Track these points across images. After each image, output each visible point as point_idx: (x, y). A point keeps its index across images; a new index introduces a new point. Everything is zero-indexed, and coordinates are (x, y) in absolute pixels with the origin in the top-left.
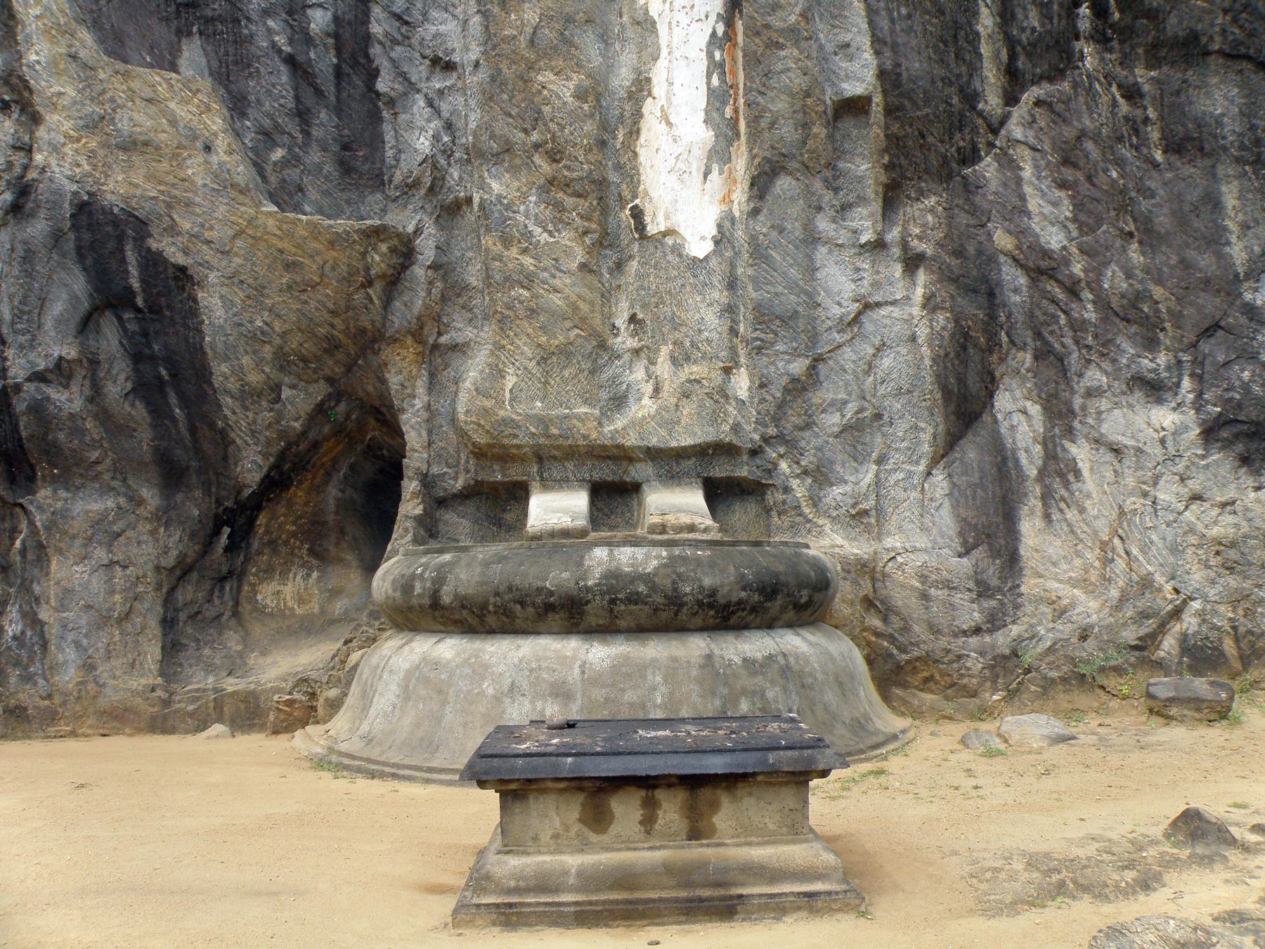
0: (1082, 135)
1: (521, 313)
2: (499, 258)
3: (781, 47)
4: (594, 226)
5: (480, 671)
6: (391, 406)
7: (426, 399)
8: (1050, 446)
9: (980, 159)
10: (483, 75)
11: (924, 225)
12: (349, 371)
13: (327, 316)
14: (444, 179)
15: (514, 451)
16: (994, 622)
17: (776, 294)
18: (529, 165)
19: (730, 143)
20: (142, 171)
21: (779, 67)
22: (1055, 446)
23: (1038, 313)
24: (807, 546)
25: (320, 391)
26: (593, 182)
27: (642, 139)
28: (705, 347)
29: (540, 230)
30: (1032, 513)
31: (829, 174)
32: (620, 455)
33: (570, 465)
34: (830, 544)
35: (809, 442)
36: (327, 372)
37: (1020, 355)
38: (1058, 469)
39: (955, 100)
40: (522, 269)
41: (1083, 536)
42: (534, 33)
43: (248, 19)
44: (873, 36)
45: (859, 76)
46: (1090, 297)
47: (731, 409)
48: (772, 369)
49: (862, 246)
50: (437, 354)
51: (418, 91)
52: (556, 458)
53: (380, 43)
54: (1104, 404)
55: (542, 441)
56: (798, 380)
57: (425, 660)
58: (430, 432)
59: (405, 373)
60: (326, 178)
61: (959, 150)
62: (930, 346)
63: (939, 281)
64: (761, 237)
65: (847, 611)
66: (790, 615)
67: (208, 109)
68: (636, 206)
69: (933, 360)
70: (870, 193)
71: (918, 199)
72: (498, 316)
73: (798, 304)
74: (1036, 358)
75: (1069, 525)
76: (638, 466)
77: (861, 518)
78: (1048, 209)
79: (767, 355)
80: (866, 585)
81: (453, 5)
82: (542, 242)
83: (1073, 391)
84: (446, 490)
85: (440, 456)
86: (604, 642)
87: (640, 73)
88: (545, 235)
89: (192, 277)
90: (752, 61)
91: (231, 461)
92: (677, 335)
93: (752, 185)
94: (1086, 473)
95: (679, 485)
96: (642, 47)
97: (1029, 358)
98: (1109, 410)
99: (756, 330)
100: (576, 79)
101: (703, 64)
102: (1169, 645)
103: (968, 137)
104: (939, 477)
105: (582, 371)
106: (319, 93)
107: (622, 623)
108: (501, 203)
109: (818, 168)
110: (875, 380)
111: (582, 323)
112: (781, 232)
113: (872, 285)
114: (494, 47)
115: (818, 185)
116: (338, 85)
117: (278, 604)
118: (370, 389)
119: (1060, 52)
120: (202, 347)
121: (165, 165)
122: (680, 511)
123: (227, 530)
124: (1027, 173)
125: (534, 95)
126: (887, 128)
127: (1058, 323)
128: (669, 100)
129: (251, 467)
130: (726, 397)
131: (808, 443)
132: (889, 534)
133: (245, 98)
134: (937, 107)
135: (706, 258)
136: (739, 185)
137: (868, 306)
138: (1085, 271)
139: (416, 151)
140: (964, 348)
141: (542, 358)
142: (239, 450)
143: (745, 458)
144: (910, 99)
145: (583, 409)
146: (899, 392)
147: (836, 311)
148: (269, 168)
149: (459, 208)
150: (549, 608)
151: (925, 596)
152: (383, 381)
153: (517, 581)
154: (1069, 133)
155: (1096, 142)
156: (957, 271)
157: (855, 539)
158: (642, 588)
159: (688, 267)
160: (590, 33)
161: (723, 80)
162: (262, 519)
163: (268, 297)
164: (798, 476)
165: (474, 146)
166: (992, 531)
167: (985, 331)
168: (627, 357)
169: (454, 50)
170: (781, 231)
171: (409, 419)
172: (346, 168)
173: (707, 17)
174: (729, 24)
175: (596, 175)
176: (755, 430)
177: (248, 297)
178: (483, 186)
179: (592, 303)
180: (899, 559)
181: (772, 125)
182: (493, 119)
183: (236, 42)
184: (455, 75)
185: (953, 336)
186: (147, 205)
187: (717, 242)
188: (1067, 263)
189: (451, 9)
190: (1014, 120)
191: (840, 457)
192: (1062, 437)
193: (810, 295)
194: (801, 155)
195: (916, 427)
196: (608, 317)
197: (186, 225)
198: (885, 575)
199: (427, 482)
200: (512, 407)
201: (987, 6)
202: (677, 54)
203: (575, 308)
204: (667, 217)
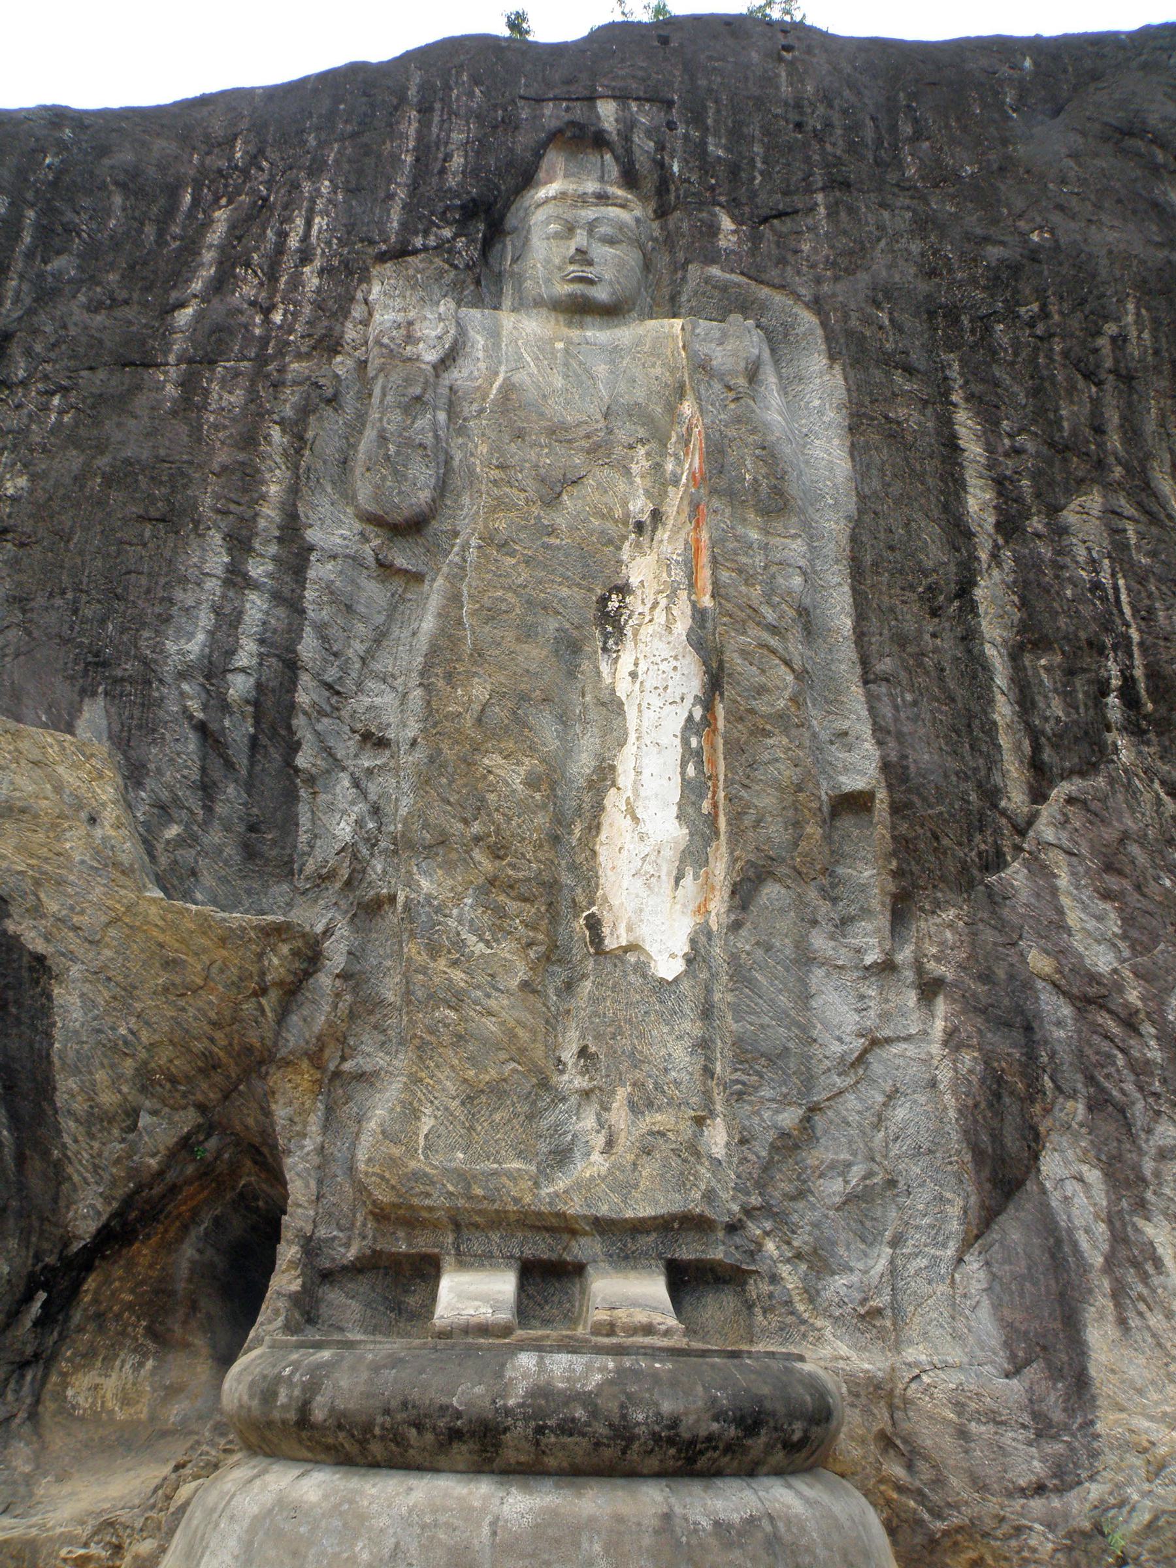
0: (1125, 837)
1: (446, 1039)
2: (424, 970)
3: (768, 734)
4: (541, 937)
5: (353, 1522)
6: (274, 1146)
7: (319, 1139)
8: (1118, 1224)
9: (1006, 865)
10: (420, 755)
11: (942, 944)
12: (226, 1097)
13: (207, 1028)
14: (364, 871)
15: (425, 1214)
17: (762, 1026)
18: (467, 861)
20: (13, 842)
21: (766, 756)
22: (1124, 1225)
23: (1088, 1051)
24: (801, 1358)
25: (187, 1120)
26: (543, 884)
27: (603, 836)
28: (671, 1091)
29: (475, 939)
31: (825, 881)
32: (562, 1227)
33: (495, 1237)
34: (832, 1356)
35: (803, 1215)
36: (199, 1097)
37: (1070, 1104)
38: (1132, 1258)
39: (973, 797)
40: (450, 985)
42: (483, 711)
43: (161, 681)
44: (875, 723)
45: (860, 769)
46: (1153, 1031)
47: (703, 1171)
48: (756, 1120)
49: (867, 968)
50: (337, 1083)
51: (344, 769)
52: (477, 1227)
53: (305, 713)
55: (461, 1202)
56: (789, 1135)
57: (281, 1502)
58: (320, 1182)
59: (296, 1104)
60: (226, 862)
61: (980, 854)
62: (954, 1093)
63: (964, 1012)
64: (744, 956)
65: (857, 1452)
66: (779, 1456)
67: (101, 776)
68: (593, 915)
69: (960, 1111)
70: (875, 904)
71: (933, 912)
72: (417, 1042)
73: (789, 1039)
74: (1090, 1108)
76: (583, 1241)
77: (873, 1319)
78: (1091, 924)
79: (750, 1103)
80: (881, 1413)
81: (393, 676)
82: (477, 953)
83: (1141, 1152)
84: (334, 1260)
85: (330, 1215)
86: (526, 1489)
87: (604, 760)
88: (481, 945)
89: (50, 968)
90: (734, 749)
91: (62, 1203)
92: (638, 1074)
93: (733, 893)
95: (634, 1268)
96: (606, 731)
97: (1081, 1108)
99: (736, 1070)
100: (529, 763)
101: (676, 752)
103: (990, 840)
104: (973, 1264)
105: (516, 1115)
106: (229, 765)
107: (551, 1462)
108: (430, 905)
109: (813, 874)
111: (520, 1054)
112: (767, 951)
113: (880, 1016)
115: (812, 894)
116: (252, 757)
117: (94, 1404)
118: (250, 1121)
119: (1091, 744)
120: (48, 1055)
121: (41, 836)
122: (634, 1304)
123: (42, 1296)
124: (1063, 881)
125: (477, 780)
126: (894, 827)
127: (1114, 1064)
128: (636, 791)
129: (86, 1214)
130: (697, 1154)
131: (802, 1217)
132: (910, 1342)
133: (144, 766)
134: (951, 804)
135: (676, 980)
136: (717, 893)
137: (875, 1043)
138: (1143, 998)
139: (334, 837)
140: (998, 1096)
141: (469, 1097)
142: (75, 1189)
143: (721, 1234)
144: (919, 795)
145: (516, 1165)
146: (917, 1152)
147: (837, 1048)
148: (160, 847)
149: (380, 907)
150: (455, 1435)
151: (963, 1434)
152: (268, 1113)
153: (415, 1394)
154: (1109, 835)
155: (1142, 845)
156: (985, 1001)
157: (865, 1349)
158: (580, 1413)
159: (653, 991)
160: (546, 714)
162: (91, 1284)
163: (139, 999)
164: (788, 1261)
165: (403, 836)
166: (1049, 1340)
167: (1023, 1074)
168: (574, 1099)
169: (389, 725)
170: (768, 948)
171: (296, 1164)
172: (250, 852)
173: (682, 699)
174: (708, 706)
175: (546, 877)
176: (734, 1198)
177: (114, 998)
178: (410, 883)
179: (533, 1031)
180: (925, 1379)
181: (758, 822)
182: (429, 805)
183: (143, 705)
184: (387, 753)
185: (982, 1081)
186: (12, 880)
187: (689, 961)
188: (1120, 989)
189: (390, 680)
190: (1043, 819)
191: (843, 1236)
192: (1132, 1212)
193: (804, 1029)
194: (792, 858)
195: (941, 1198)
196: (553, 1049)
197: (52, 907)
198: (907, 1402)
199: (310, 1247)
200: (427, 1157)
201: (1003, 693)
202: (647, 740)
203: (512, 1035)
204: (630, 929)
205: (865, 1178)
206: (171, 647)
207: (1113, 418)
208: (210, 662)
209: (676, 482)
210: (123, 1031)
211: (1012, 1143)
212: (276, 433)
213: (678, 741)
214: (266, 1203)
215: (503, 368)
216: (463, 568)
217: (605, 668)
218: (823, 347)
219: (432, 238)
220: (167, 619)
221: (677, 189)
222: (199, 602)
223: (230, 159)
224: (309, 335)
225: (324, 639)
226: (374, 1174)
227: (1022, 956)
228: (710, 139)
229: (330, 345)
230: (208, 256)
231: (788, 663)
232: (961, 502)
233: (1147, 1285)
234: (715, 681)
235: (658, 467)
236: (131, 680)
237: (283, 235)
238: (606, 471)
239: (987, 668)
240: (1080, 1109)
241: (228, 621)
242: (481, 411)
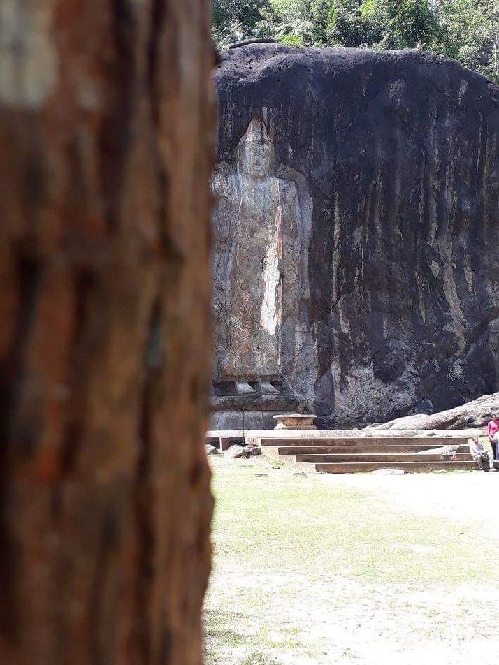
16: (330, 413)
35: (293, 374)
38: (344, 382)
102: (365, 419)
207: (369, 206)
211: (327, 364)
217: (263, 275)
234: (282, 276)
239: (333, 272)
240: (338, 357)
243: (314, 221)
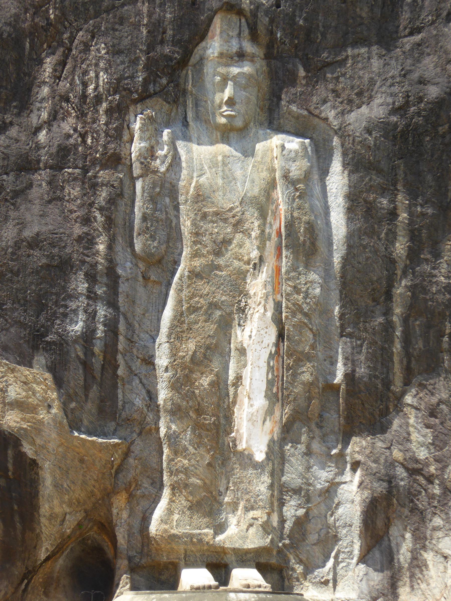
0: (441, 402)
13: (93, 482)
17: (292, 478)
19: (274, 404)
30: (405, 585)
32: (222, 551)
39: (380, 386)
41: (428, 596)
54: (440, 534)
69: (361, 512)
73: (302, 484)
75: (422, 591)
78: (421, 439)
89: (38, 464)
92: (248, 497)
94: (431, 566)
98: (443, 537)
101: (265, 369)
106: (94, 377)
110: (335, 519)
114: (174, 361)
116: (102, 374)
118: (102, 514)
123: (26, 581)
124: (412, 421)
138: (436, 469)
147: (319, 486)
152: (110, 511)
154: (434, 400)
155: (447, 406)
156: (375, 471)
161: (273, 375)
173: (268, 345)
174: (277, 345)
192: (420, 549)
204: (247, 442)
205: (326, 534)
206: (69, 328)
208: (86, 335)
209: (269, 239)
210: (65, 486)
211: (380, 523)
212: (97, 214)
213: (266, 364)
214: (92, 541)
215: (195, 175)
216: (182, 286)
217: (239, 332)
218: (341, 159)
219: (158, 85)
220: (65, 315)
221: (278, 48)
222: (78, 307)
223: (48, 19)
224: (106, 153)
225: (126, 318)
226: (159, 535)
227: (391, 453)
228: (297, 13)
229: (115, 160)
230: (46, 90)
231: (311, 330)
232: (394, 246)
233: (422, 574)
235: (263, 232)
236: (54, 343)
237: (85, 85)
238: (241, 235)
241: (92, 316)
242: (186, 201)
243: (349, 220)
